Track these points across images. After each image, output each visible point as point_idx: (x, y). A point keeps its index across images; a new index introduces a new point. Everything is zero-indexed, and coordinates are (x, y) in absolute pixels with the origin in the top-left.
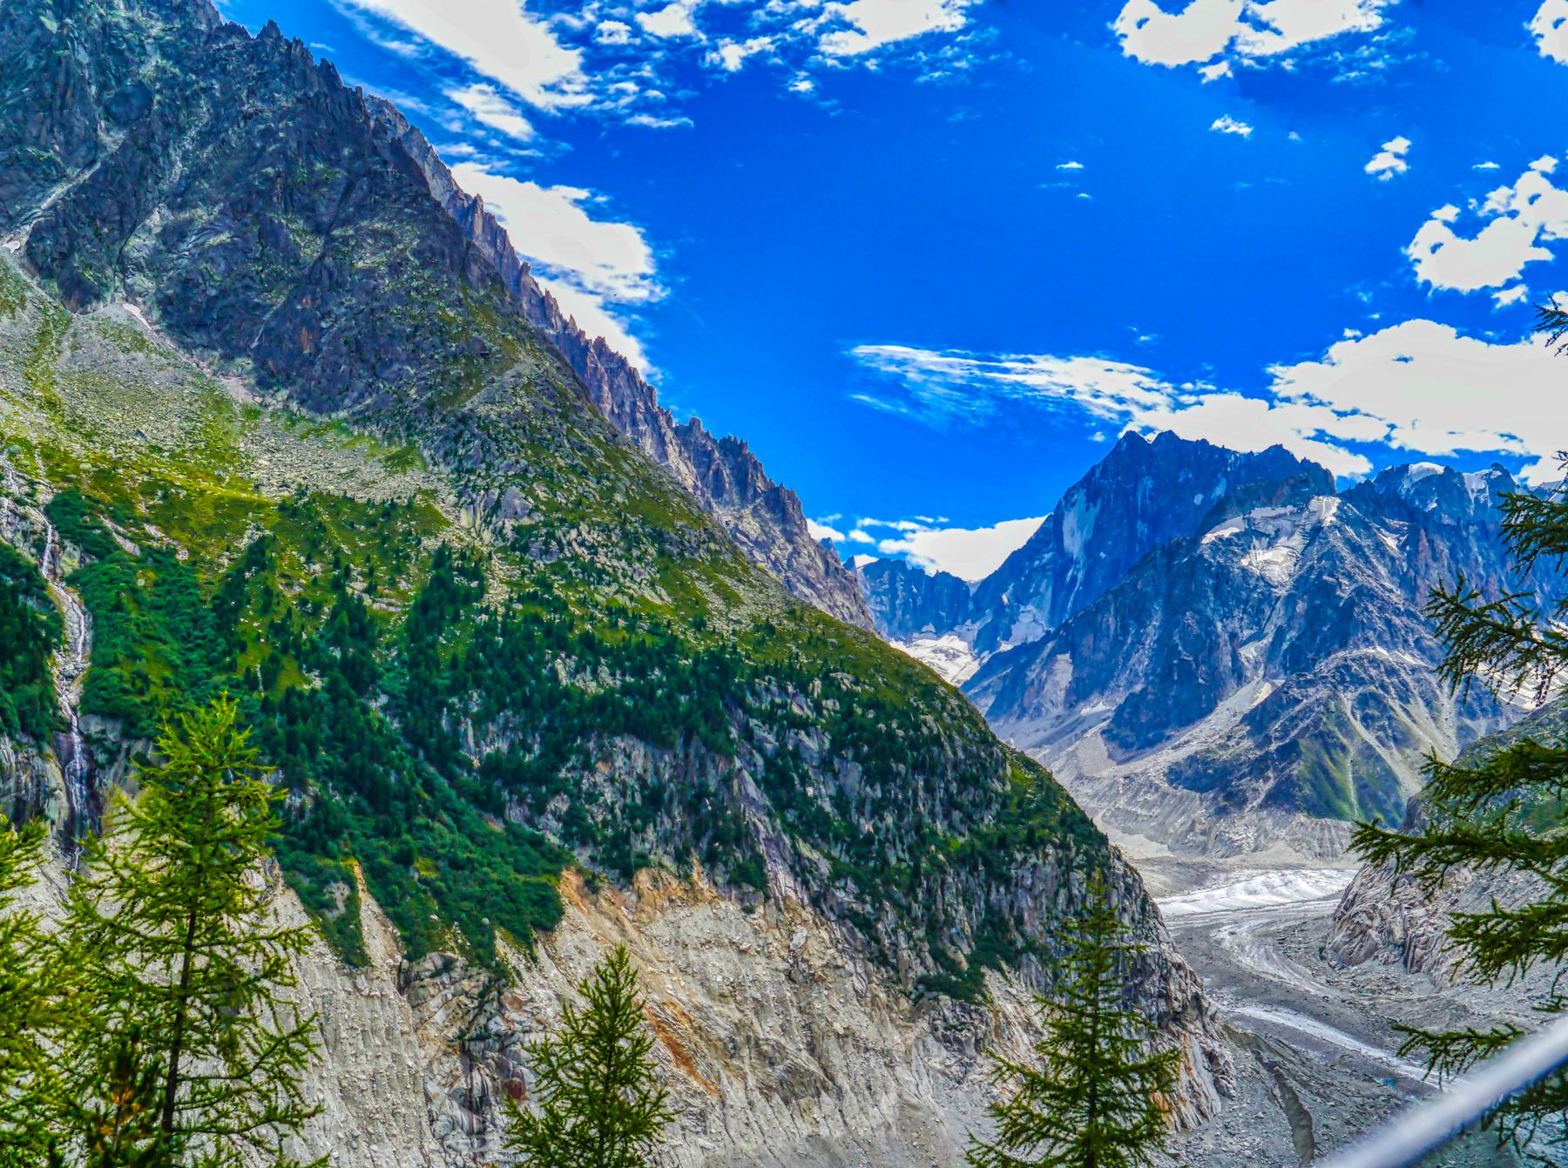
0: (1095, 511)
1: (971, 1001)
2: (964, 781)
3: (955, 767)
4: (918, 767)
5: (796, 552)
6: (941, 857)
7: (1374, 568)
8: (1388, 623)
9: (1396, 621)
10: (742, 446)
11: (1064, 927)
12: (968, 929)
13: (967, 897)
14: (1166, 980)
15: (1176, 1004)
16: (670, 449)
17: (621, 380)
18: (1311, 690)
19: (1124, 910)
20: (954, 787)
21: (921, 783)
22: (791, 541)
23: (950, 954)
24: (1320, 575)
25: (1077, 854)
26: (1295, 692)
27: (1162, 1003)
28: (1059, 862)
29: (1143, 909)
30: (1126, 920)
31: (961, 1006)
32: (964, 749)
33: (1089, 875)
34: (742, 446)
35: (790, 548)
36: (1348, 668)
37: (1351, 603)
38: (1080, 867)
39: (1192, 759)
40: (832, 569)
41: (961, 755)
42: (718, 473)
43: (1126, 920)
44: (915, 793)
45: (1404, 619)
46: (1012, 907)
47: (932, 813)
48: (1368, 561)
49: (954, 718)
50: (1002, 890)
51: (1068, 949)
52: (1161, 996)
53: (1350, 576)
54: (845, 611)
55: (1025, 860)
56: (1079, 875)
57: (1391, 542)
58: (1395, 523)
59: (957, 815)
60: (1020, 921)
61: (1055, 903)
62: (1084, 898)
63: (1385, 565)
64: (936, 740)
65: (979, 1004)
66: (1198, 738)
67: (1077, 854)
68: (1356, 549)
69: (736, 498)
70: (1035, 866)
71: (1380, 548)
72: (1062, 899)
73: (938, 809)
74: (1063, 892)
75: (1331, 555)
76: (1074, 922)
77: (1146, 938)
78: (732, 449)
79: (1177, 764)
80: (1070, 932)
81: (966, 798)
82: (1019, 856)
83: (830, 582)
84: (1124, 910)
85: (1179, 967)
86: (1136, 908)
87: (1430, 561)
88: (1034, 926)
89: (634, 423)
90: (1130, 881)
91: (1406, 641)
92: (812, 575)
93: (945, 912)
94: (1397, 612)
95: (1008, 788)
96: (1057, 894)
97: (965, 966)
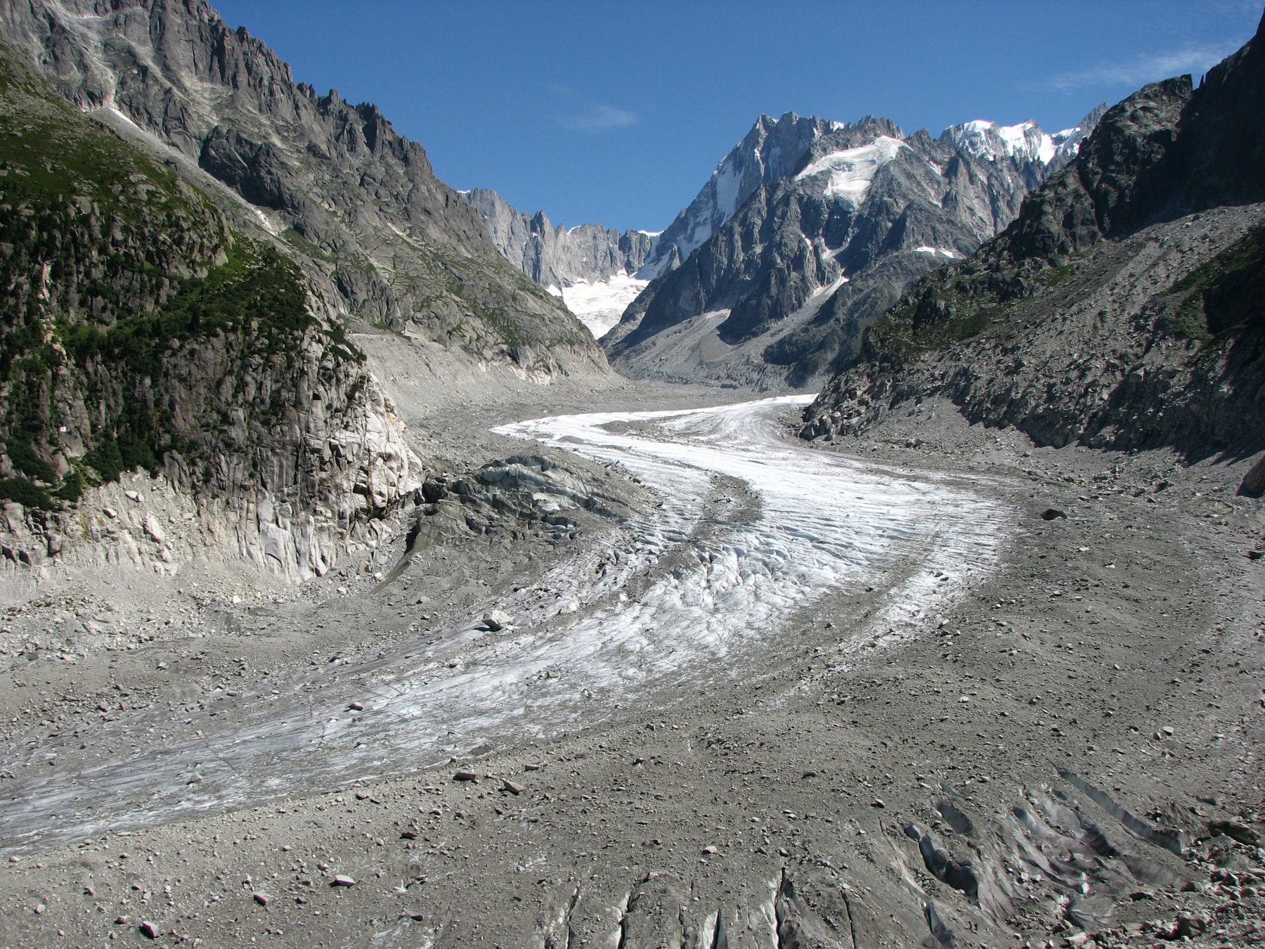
0: (740, 176)
1: (47, 506)
2: (113, 266)
3: (103, 251)
4: (43, 250)
5: (416, 187)
6: (57, 346)
7: (924, 190)
8: (934, 229)
9: (939, 227)
10: (373, 109)
11: (226, 419)
12: (87, 427)
13: (93, 395)
14: (366, 472)
15: (378, 499)
16: (303, 112)
17: (260, 60)
18: (871, 282)
19: (316, 397)
20: (97, 273)
21: (47, 269)
22: (412, 181)
23: (46, 458)
24: (882, 196)
25: (257, 338)
26: (859, 284)
27: (361, 497)
28: (229, 346)
29: (350, 397)
30: (319, 410)
31: (34, 514)
32: (126, 229)
33: (267, 360)
34: (373, 109)
35: (411, 185)
36: (900, 263)
37: (904, 217)
38: (259, 352)
39: (781, 343)
40: (451, 201)
41: (119, 236)
42: (351, 132)
43: (319, 410)
44: (36, 281)
45: (946, 225)
46: (158, 403)
47: (64, 303)
48: (919, 184)
49: (130, 200)
50: (148, 381)
51: (229, 445)
52: (357, 490)
53: (905, 197)
54: (461, 233)
55: (182, 347)
56: (257, 360)
57: (937, 170)
58: (938, 155)
59: (99, 301)
60: (167, 419)
61: (218, 393)
62: (260, 387)
63: (933, 188)
64: (85, 220)
65: (61, 509)
66: (789, 325)
67: (257, 338)
68: (910, 176)
69: (366, 149)
70: (192, 352)
71: (929, 174)
72: (227, 390)
73: (75, 297)
74: (230, 381)
75: (892, 180)
76: (241, 414)
77: (346, 427)
78: (368, 113)
79: (771, 347)
80: (232, 424)
81: (119, 283)
82: (176, 343)
83: (449, 212)
84: (316, 397)
85: (387, 458)
86: (336, 395)
87: (968, 183)
88: (184, 422)
89: (272, 93)
90: (330, 365)
91: (946, 242)
92: (429, 206)
93: (54, 408)
94: (940, 221)
95: (203, 274)
96: (219, 383)
97: (64, 467)
